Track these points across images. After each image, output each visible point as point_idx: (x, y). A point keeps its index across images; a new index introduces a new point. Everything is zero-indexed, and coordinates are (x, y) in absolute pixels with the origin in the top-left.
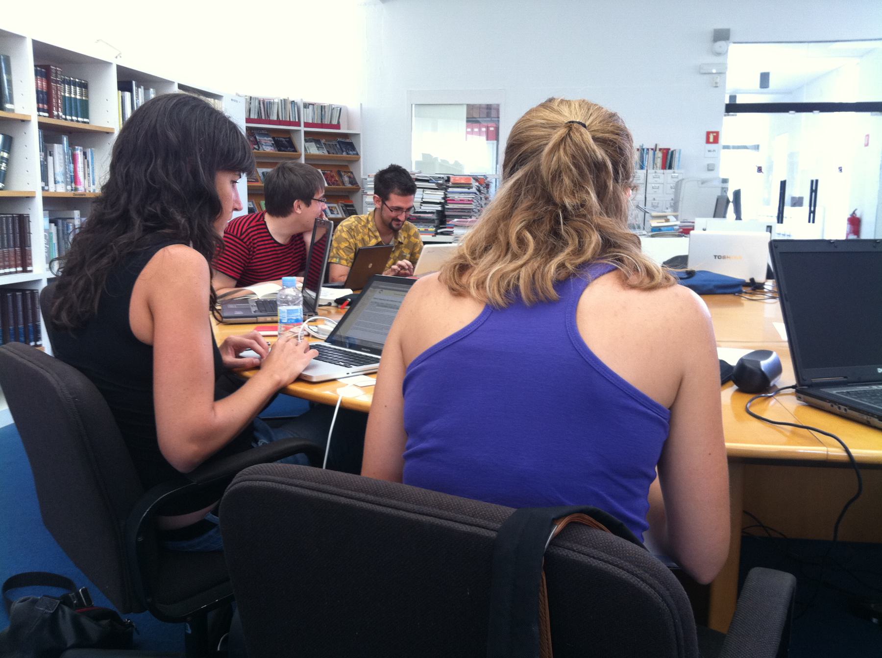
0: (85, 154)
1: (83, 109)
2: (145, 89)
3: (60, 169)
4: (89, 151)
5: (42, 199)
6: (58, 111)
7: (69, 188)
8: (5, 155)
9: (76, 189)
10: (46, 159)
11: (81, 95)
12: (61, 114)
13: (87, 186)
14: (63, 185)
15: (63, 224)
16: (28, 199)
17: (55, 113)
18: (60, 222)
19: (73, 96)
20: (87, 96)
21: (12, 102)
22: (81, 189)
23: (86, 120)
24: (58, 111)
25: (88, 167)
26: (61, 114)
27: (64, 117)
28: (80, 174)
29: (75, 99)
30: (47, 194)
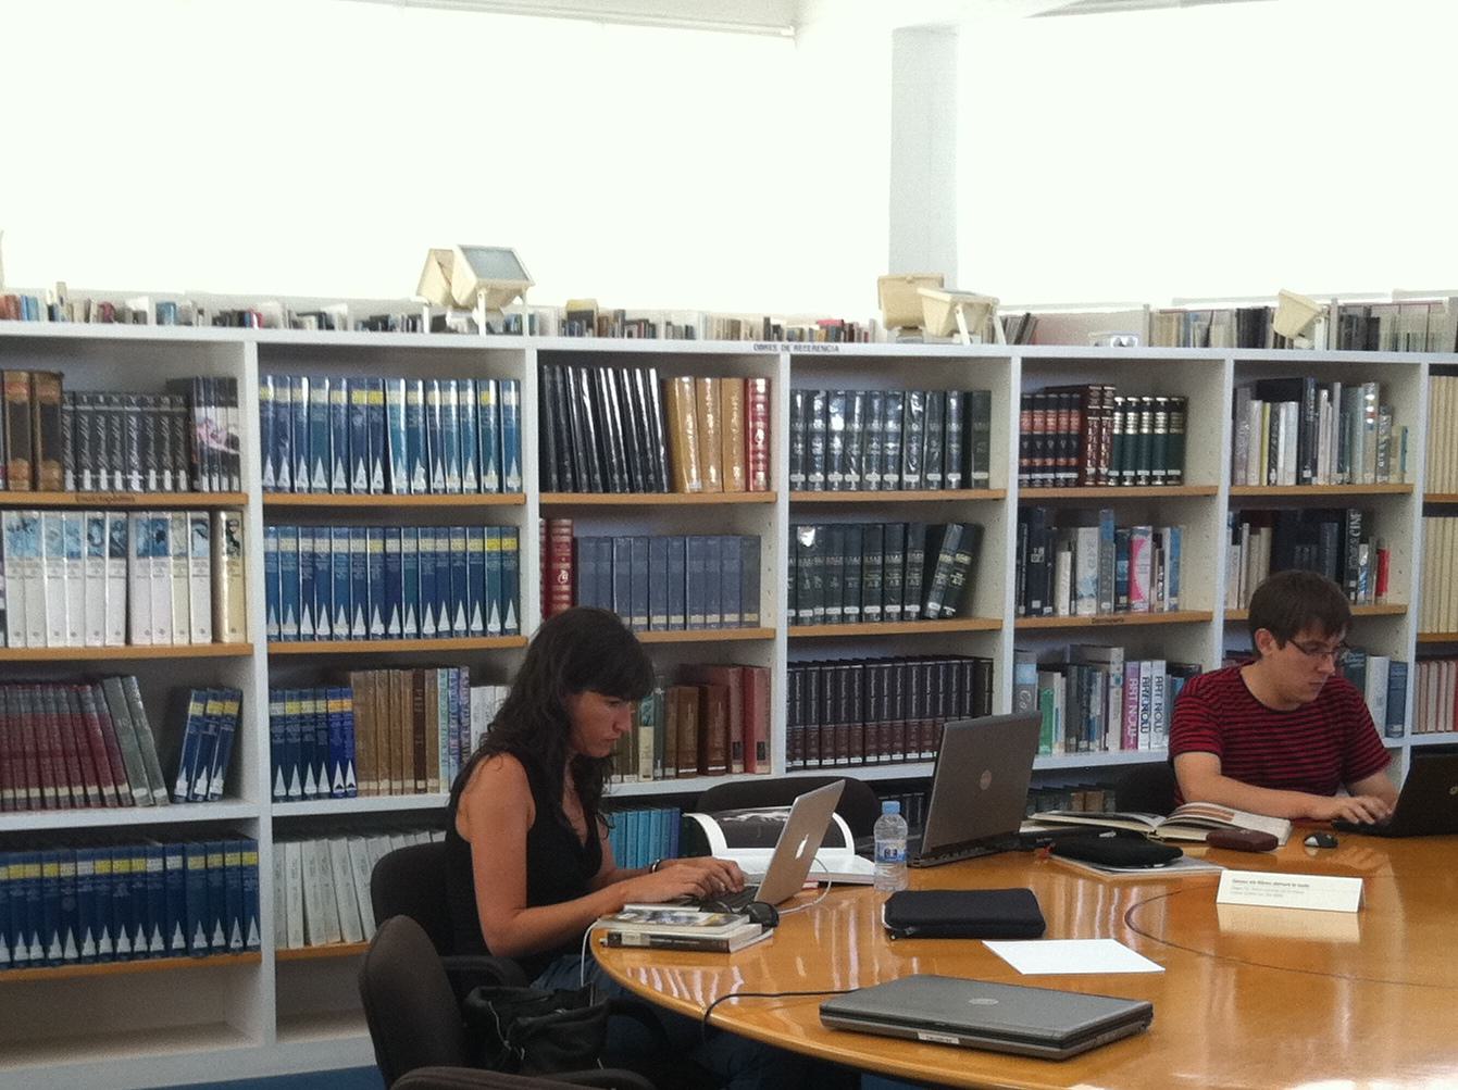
0: (1157, 540)
1: (1172, 451)
2: (1344, 387)
3: (1088, 572)
4: (1167, 532)
5: (1013, 632)
6: (1097, 465)
7: (1106, 605)
8: (965, 559)
9: (1128, 607)
10: (1052, 558)
11: (1168, 425)
12: (1104, 470)
13: (1154, 599)
14: (1094, 602)
15: (1080, 675)
16: (994, 632)
17: (1091, 470)
18: (1074, 669)
19: (1130, 431)
20: (1184, 425)
21: (985, 467)
22: (1140, 606)
23: (1171, 472)
24: (1097, 465)
25: (1162, 562)
26: (1104, 470)
27: (1116, 473)
28: (1142, 580)
29: (1152, 436)
30: (1033, 622)
